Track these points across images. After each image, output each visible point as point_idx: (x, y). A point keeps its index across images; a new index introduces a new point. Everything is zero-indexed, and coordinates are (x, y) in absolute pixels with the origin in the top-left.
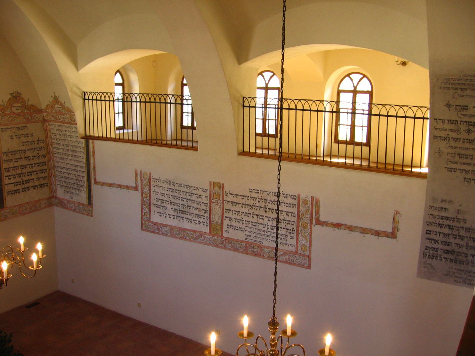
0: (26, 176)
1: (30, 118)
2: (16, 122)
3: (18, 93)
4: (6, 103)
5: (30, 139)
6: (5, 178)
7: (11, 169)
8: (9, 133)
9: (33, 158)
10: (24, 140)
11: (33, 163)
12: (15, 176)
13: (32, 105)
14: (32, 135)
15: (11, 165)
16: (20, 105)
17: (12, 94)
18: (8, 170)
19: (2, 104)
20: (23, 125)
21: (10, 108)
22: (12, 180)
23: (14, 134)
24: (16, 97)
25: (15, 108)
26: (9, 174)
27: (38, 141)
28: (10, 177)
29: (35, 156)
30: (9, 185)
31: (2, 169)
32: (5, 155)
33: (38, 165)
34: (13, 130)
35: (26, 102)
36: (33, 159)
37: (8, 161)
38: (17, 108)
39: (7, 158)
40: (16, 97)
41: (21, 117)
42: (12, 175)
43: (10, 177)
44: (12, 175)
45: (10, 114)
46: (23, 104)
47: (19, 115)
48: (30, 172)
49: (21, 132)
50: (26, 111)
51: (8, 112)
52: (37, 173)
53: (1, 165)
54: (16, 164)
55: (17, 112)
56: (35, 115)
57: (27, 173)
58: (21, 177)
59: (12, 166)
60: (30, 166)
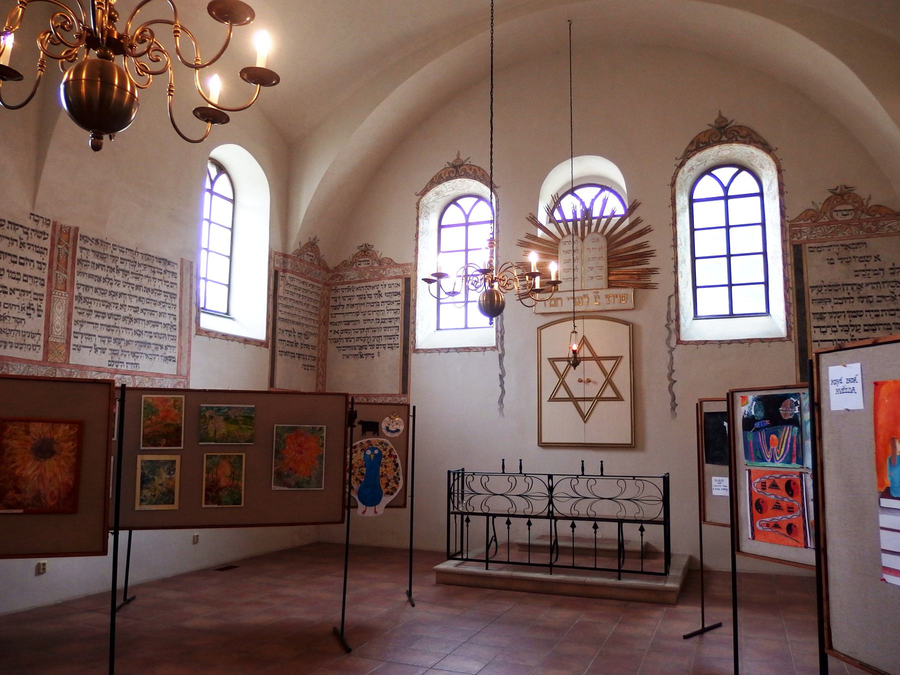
0: (862, 330)
1: (874, 228)
2: (840, 235)
3: (846, 188)
4: (820, 207)
5: (872, 265)
6: (813, 330)
7: (827, 316)
8: (825, 254)
9: (879, 299)
10: (861, 266)
11: (880, 308)
12: (834, 329)
13: (879, 206)
14: (877, 258)
15: (828, 308)
16: (849, 207)
17: (833, 191)
18: (821, 316)
19: (813, 207)
20: (856, 241)
21: (828, 214)
22: (828, 334)
23: (835, 257)
24: (841, 195)
25: (840, 214)
26: (821, 323)
27: (891, 269)
28: (824, 330)
29: (883, 297)
30: (821, 344)
31: (807, 314)
32: (815, 291)
33: (892, 312)
34: (835, 249)
35: (865, 202)
36: (879, 301)
37: (820, 301)
38: (845, 213)
39: (820, 296)
40: (841, 195)
41: (853, 228)
42: (828, 327)
43: (824, 330)
44: (828, 327)
45: (828, 224)
46: (856, 205)
47: (848, 224)
48: (870, 325)
49: (852, 253)
50: (864, 216)
51: (825, 219)
52: (890, 329)
53: (807, 307)
54: (838, 308)
55: (844, 218)
56: (886, 222)
57: (865, 325)
58: (850, 332)
59: (830, 310)
60: (873, 314)
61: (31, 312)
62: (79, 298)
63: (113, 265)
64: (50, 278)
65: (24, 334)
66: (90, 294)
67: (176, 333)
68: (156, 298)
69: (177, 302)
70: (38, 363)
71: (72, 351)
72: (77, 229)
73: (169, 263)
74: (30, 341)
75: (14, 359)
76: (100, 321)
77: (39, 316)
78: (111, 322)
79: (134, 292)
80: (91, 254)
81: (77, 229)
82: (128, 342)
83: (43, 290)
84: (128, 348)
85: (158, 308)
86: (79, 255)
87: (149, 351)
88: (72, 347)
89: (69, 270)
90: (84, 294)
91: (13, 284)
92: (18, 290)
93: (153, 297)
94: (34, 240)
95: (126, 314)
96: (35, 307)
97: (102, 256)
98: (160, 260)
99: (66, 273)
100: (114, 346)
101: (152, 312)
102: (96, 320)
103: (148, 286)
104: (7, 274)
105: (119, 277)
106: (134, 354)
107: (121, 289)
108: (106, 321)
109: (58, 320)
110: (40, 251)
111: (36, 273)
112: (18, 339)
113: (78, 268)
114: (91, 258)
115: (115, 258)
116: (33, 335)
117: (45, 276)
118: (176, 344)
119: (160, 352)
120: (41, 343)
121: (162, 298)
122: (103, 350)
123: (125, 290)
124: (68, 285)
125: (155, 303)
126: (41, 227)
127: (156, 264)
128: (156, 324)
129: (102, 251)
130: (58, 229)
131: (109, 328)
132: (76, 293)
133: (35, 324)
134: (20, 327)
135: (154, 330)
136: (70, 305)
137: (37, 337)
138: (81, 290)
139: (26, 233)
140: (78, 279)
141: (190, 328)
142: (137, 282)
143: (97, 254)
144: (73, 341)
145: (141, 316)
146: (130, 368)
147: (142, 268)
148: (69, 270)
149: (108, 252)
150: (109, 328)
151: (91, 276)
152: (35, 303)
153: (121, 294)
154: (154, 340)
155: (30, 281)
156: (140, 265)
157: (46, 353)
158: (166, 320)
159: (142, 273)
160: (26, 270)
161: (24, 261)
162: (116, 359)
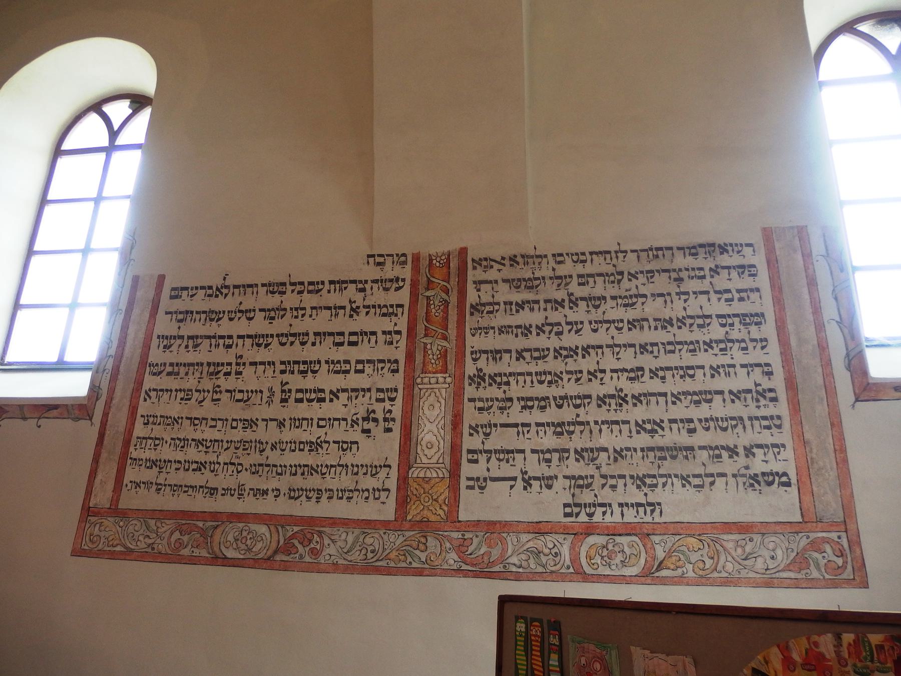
61: (371, 425)
62: (479, 378)
63: (560, 295)
64: (410, 356)
65: (355, 470)
66: (507, 365)
67: (782, 409)
68: (698, 335)
69: (769, 330)
70: (386, 525)
71: (463, 492)
72: (463, 251)
73: (723, 249)
74: (369, 483)
75: (334, 522)
76: (536, 416)
77: (389, 430)
78: (567, 414)
79: (624, 337)
80: (503, 287)
81: (463, 251)
82: (619, 454)
83: (398, 380)
84: (623, 468)
85: (705, 358)
86: (472, 296)
87: (693, 467)
88: (464, 483)
89: (452, 332)
90: (490, 368)
91: (338, 382)
92: (344, 390)
93: (684, 335)
94: (378, 296)
95: (609, 388)
96: (380, 415)
97: (531, 284)
98: (692, 250)
99: (445, 338)
100: (574, 467)
101: (687, 372)
102: (525, 417)
103: (667, 314)
104: (325, 367)
105: (580, 314)
106: (640, 481)
107: (587, 338)
108: (552, 414)
109: (431, 431)
110: (388, 312)
111: (382, 351)
112: (346, 481)
113: (470, 322)
114: (504, 294)
115: (561, 280)
116: (374, 470)
117: (401, 356)
118: (785, 436)
119: (728, 465)
120: (392, 484)
121: (716, 332)
122: (548, 482)
123: (602, 337)
124: (451, 362)
125: (693, 347)
126: (390, 272)
127: (681, 261)
128: (704, 397)
129: (528, 275)
130: (424, 263)
131: (560, 429)
132: (470, 369)
133: (386, 447)
134: (348, 459)
135: (704, 411)
136: (458, 395)
137: (383, 473)
138: (482, 363)
139: (363, 290)
140: (473, 342)
141: (830, 390)
142: (631, 314)
143: (514, 284)
144: (467, 470)
145: (655, 386)
146: (630, 516)
147: (642, 279)
148: (452, 332)
149: (546, 272)
150: (560, 429)
151: (504, 330)
152: (379, 407)
153: (586, 350)
154: (702, 438)
155: (368, 369)
156: (633, 276)
157: (403, 503)
158: (741, 381)
159: (643, 290)
160: (364, 351)
161: (355, 339)
162: (587, 497)
